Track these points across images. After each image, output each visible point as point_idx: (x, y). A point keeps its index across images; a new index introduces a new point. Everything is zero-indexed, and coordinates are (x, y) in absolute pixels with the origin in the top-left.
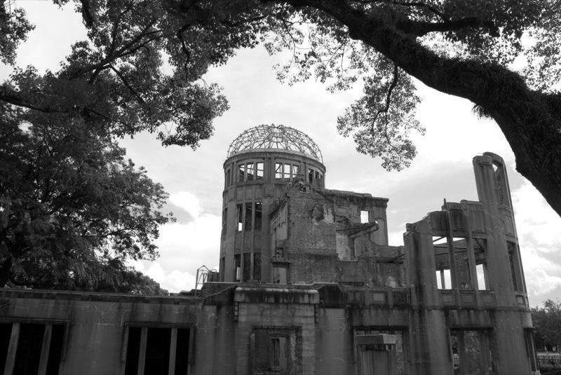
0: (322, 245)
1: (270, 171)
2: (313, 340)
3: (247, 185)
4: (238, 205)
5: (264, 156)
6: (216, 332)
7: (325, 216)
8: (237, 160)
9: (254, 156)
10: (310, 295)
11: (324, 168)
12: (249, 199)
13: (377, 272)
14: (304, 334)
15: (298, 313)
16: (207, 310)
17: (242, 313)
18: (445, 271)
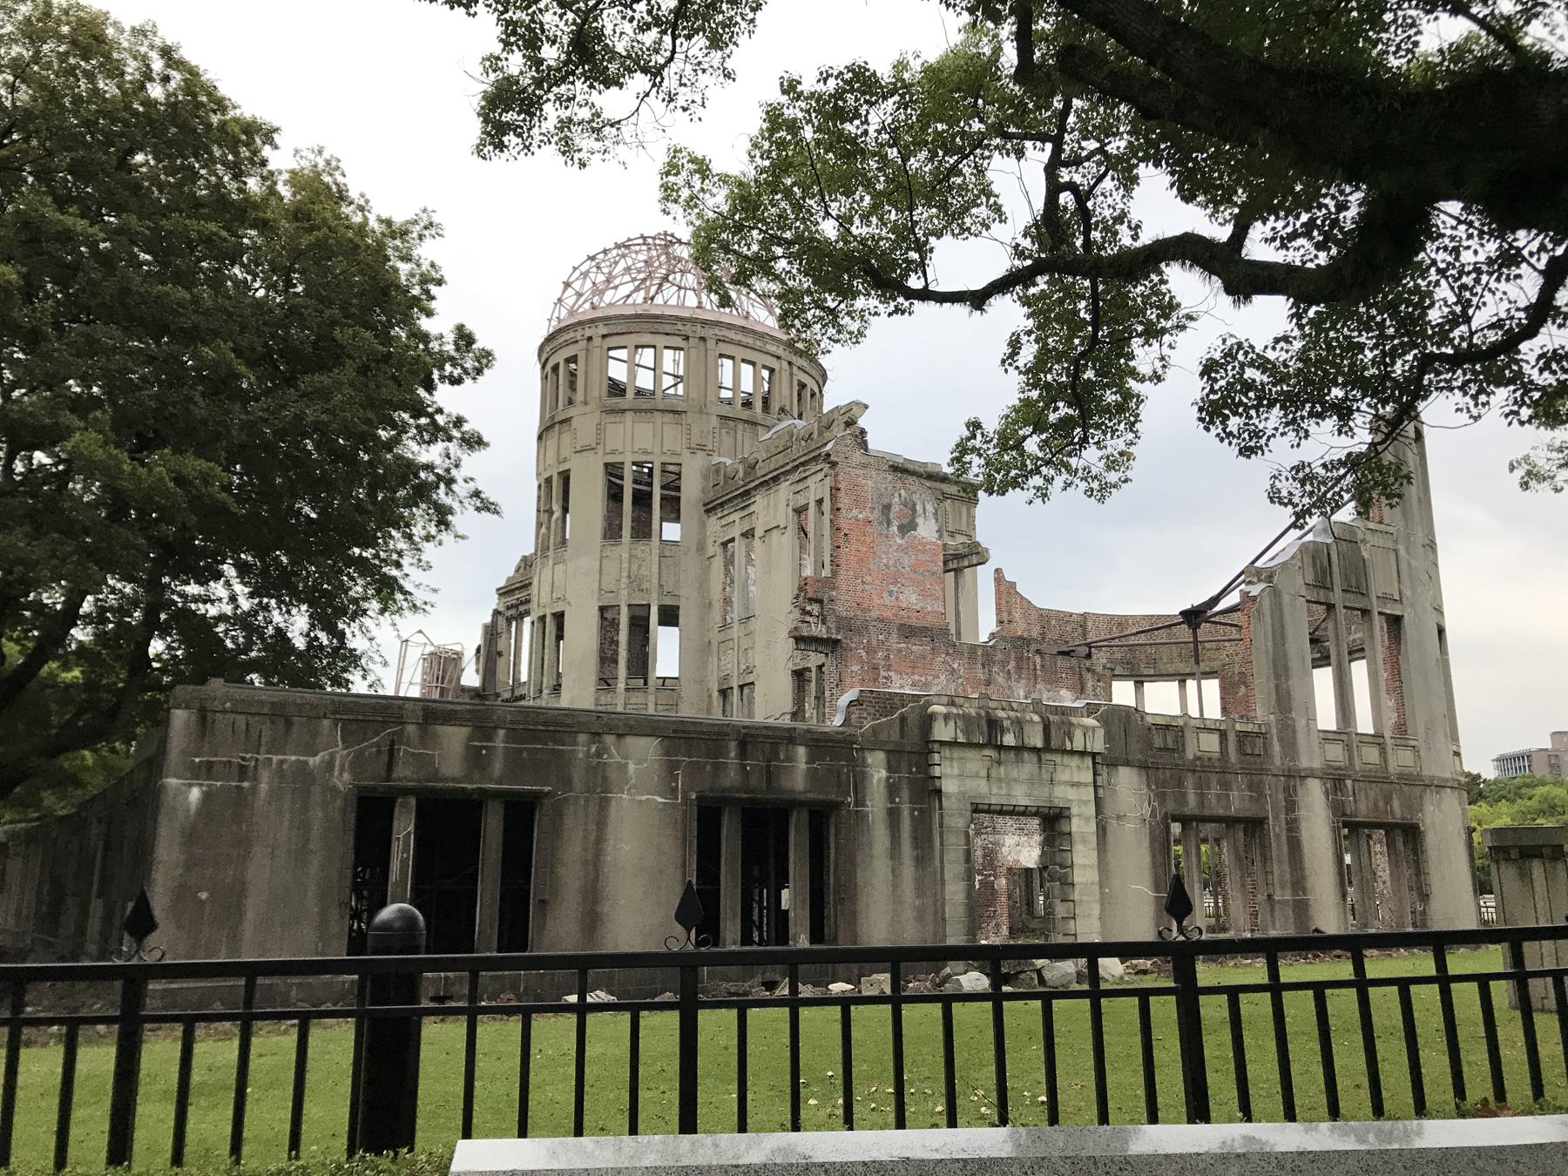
0: (913, 599)
1: (702, 375)
3: (635, 411)
4: (606, 465)
5: (687, 329)
6: (893, 815)
7: (920, 521)
8: (603, 330)
9: (660, 328)
10: (1086, 729)
12: (645, 452)
13: (1035, 675)
14: (1076, 825)
15: (1063, 775)
16: (869, 761)
17: (948, 771)
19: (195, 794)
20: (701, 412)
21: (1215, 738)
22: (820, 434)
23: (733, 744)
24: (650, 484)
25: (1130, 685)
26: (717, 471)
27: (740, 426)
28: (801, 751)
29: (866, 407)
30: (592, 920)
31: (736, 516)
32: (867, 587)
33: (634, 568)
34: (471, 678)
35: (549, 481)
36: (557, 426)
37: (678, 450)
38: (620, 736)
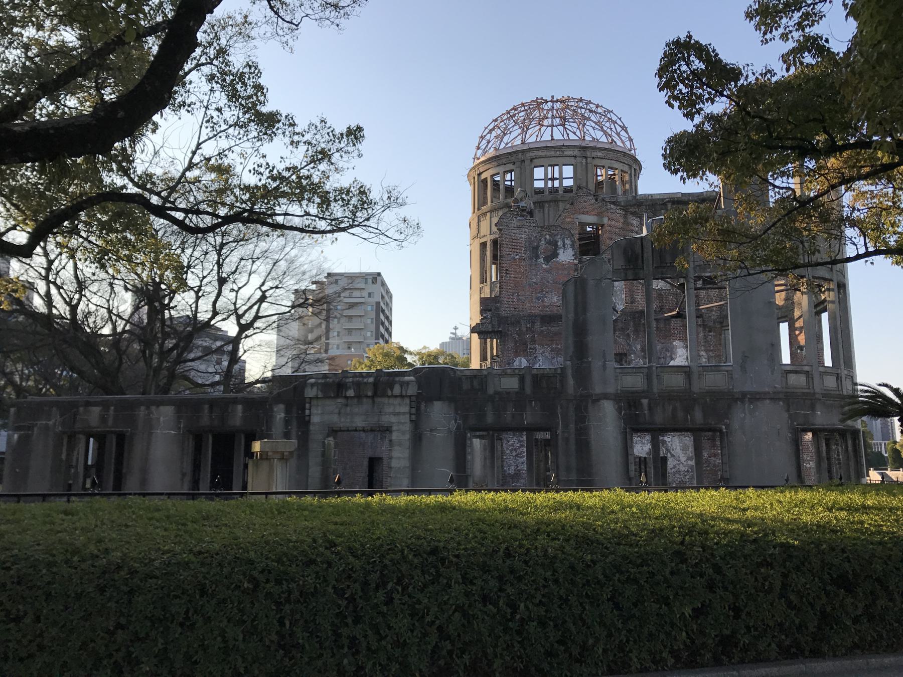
2: (407, 444)
5: (513, 159)
7: (561, 251)
16: (275, 409)
19: (16, 436)
23: (206, 407)
28: (240, 408)
30: (144, 482)
32: (521, 297)
38: (158, 406)
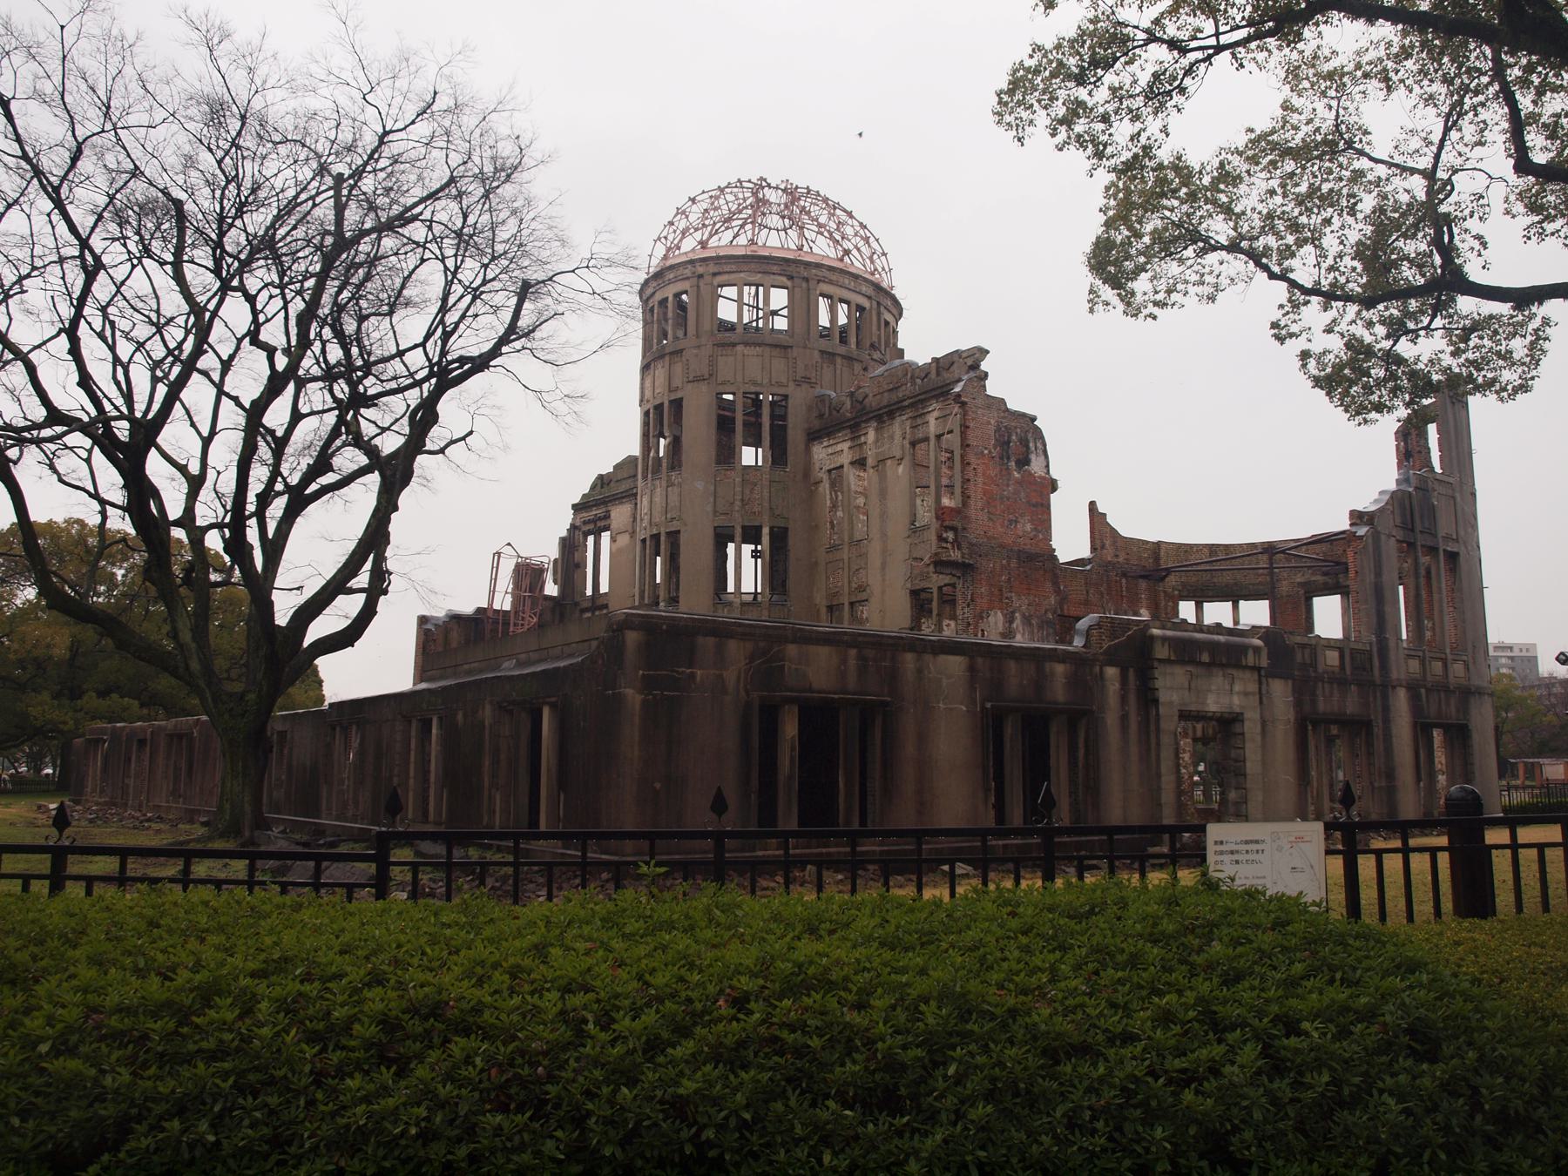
2: (1259, 738)
5: (791, 269)
6: (1124, 718)
7: (1033, 457)
8: (712, 268)
9: (768, 268)
10: (1257, 650)
11: (901, 315)
12: (755, 384)
18: (1242, 603)
20: (805, 347)
21: (1336, 654)
22: (938, 374)
24: (734, 411)
25: (1192, 604)
26: (823, 401)
27: (839, 360)
29: (988, 352)
31: (845, 446)
33: (747, 492)
34: (551, 589)
35: (659, 408)
36: (667, 358)
37: (784, 380)
